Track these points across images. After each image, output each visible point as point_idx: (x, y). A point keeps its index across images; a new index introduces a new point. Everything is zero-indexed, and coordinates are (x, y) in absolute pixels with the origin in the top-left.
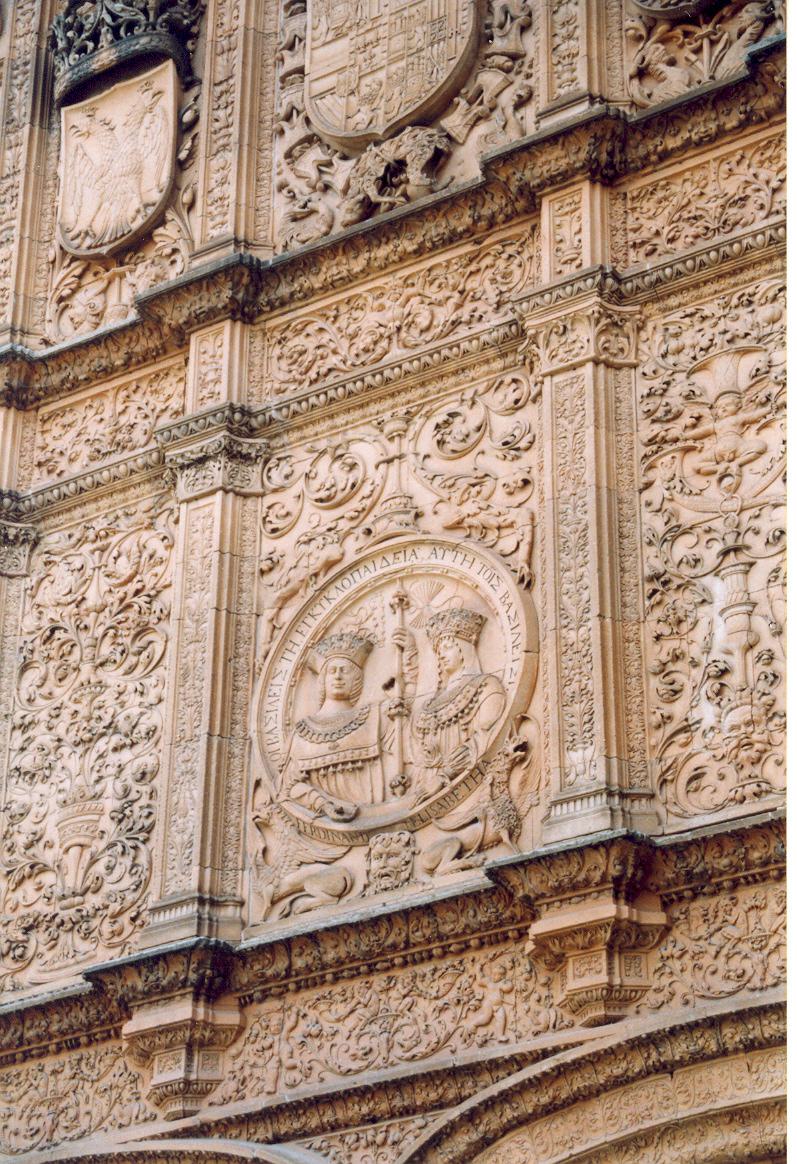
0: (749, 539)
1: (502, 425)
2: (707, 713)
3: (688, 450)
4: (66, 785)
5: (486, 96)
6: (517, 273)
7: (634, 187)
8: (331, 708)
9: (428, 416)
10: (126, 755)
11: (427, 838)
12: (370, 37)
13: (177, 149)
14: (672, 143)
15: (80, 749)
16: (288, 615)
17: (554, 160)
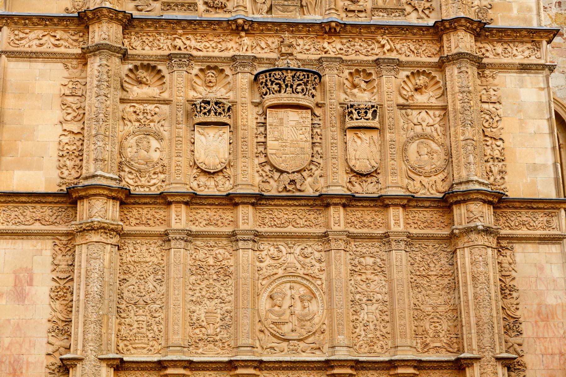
0: (372, 298)
1: (317, 255)
2: (363, 333)
3: (360, 275)
4: (206, 307)
5: (313, 171)
6: (320, 219)
7: (348, 209)
8: (277, 308)
9: (299, 245)
10: (223, 305)
11: (302, 345)
12: (284, 144)
13: (230, 149)
14: (359, 204)
15: (211, 300)
16: (264, 282)
17: (336, 201)
